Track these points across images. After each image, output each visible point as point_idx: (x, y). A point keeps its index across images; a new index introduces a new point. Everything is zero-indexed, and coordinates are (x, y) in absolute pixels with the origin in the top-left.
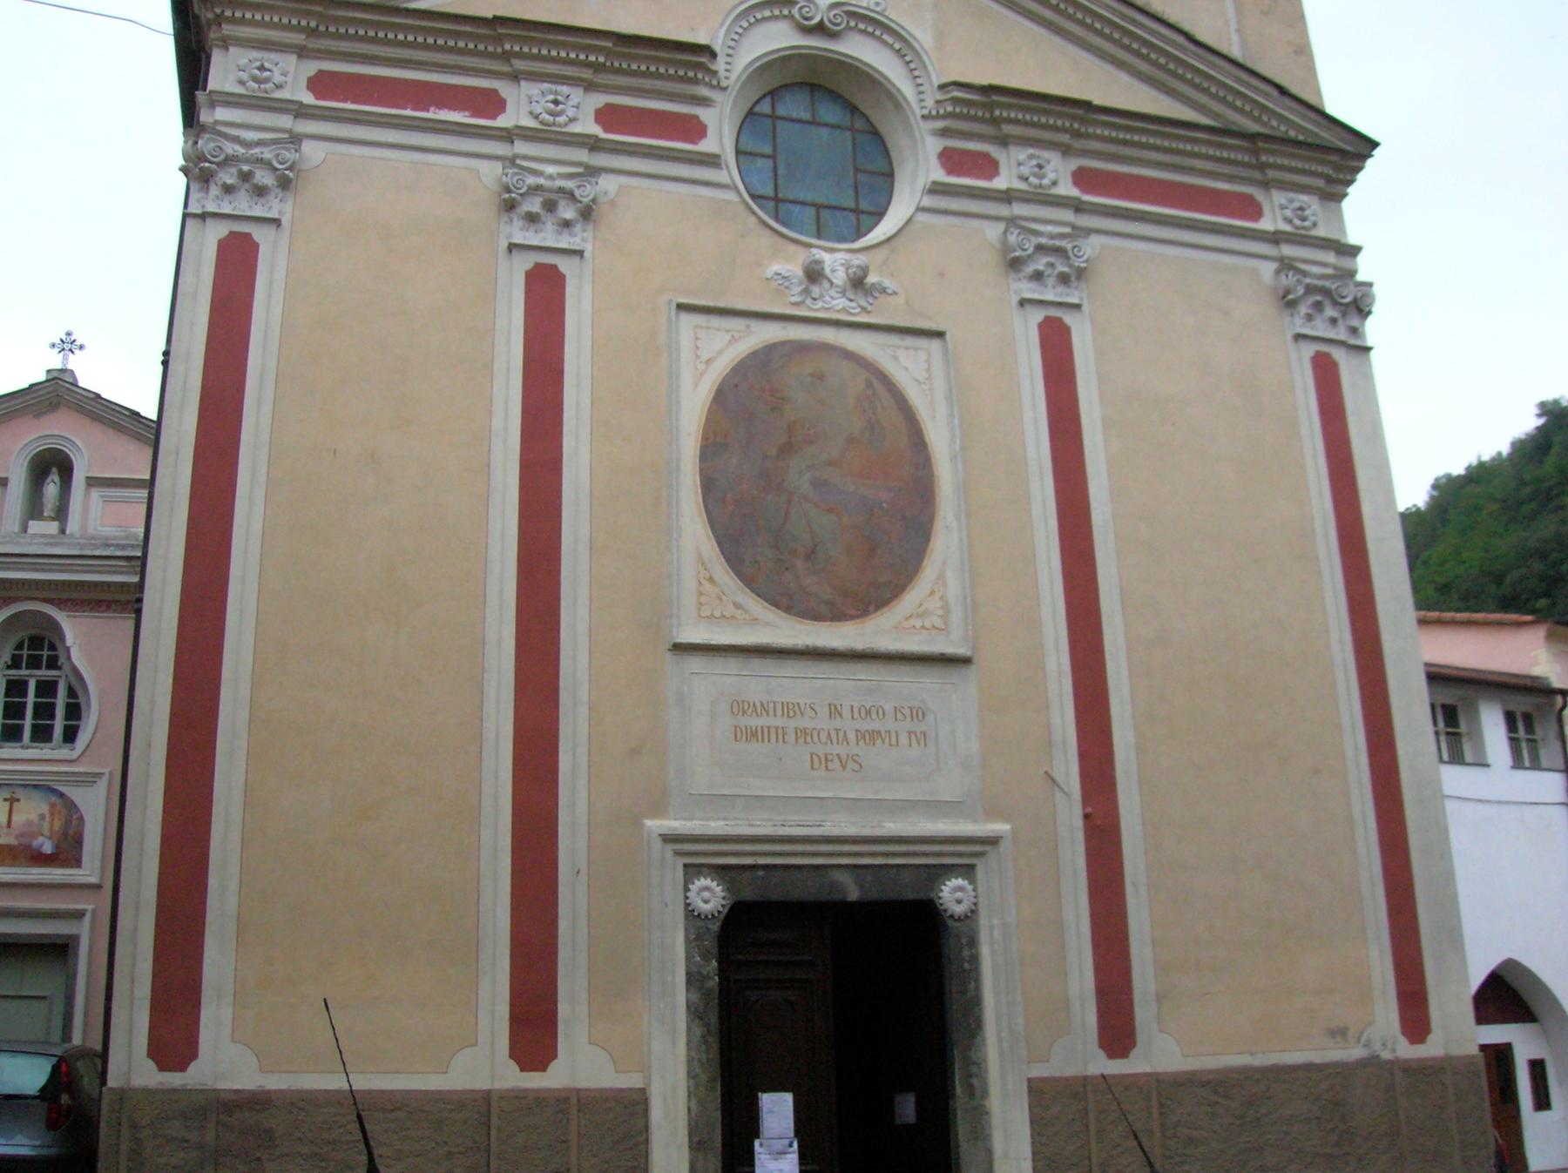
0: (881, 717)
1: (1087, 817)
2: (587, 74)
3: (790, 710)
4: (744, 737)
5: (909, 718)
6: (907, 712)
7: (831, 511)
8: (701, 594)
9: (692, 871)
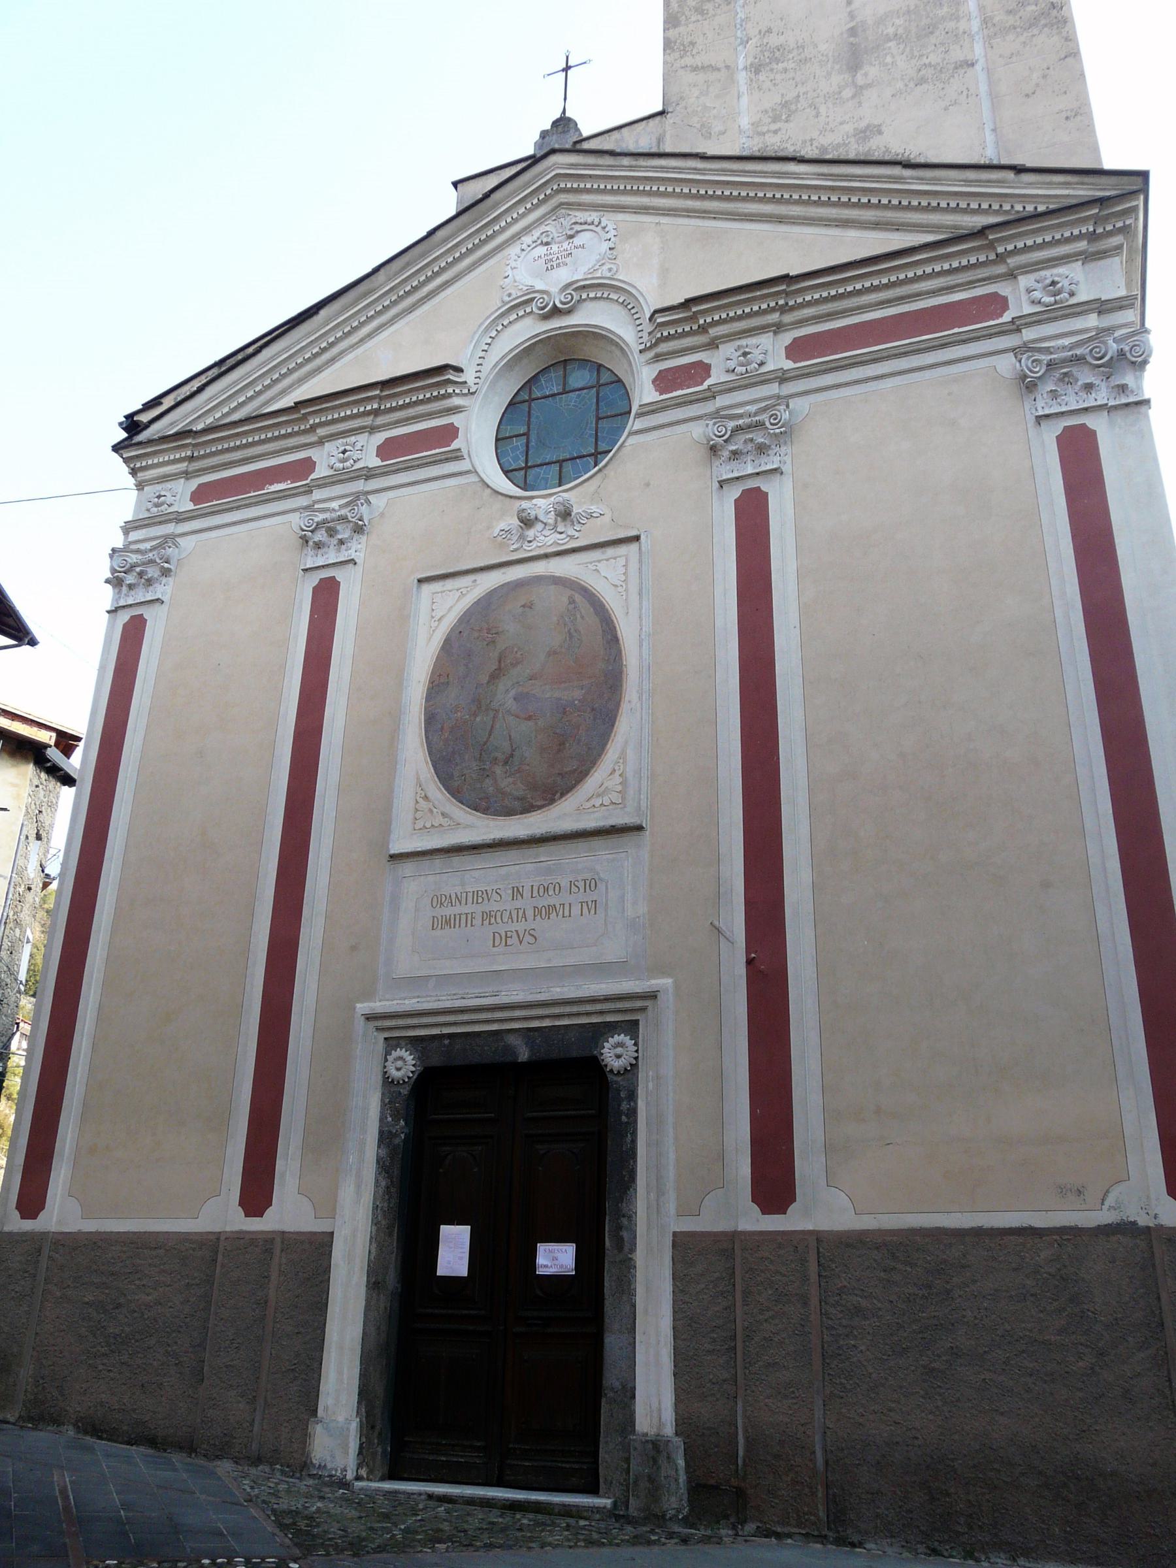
0: (557, 892)
1: (749, 962)
2: (368, 421)
3: (480, 896)
4: (440, 926)
5: (582, 890)
6: (581, 885)
7: (529, 718)
8: (417, 810)
9: (392, 1044)
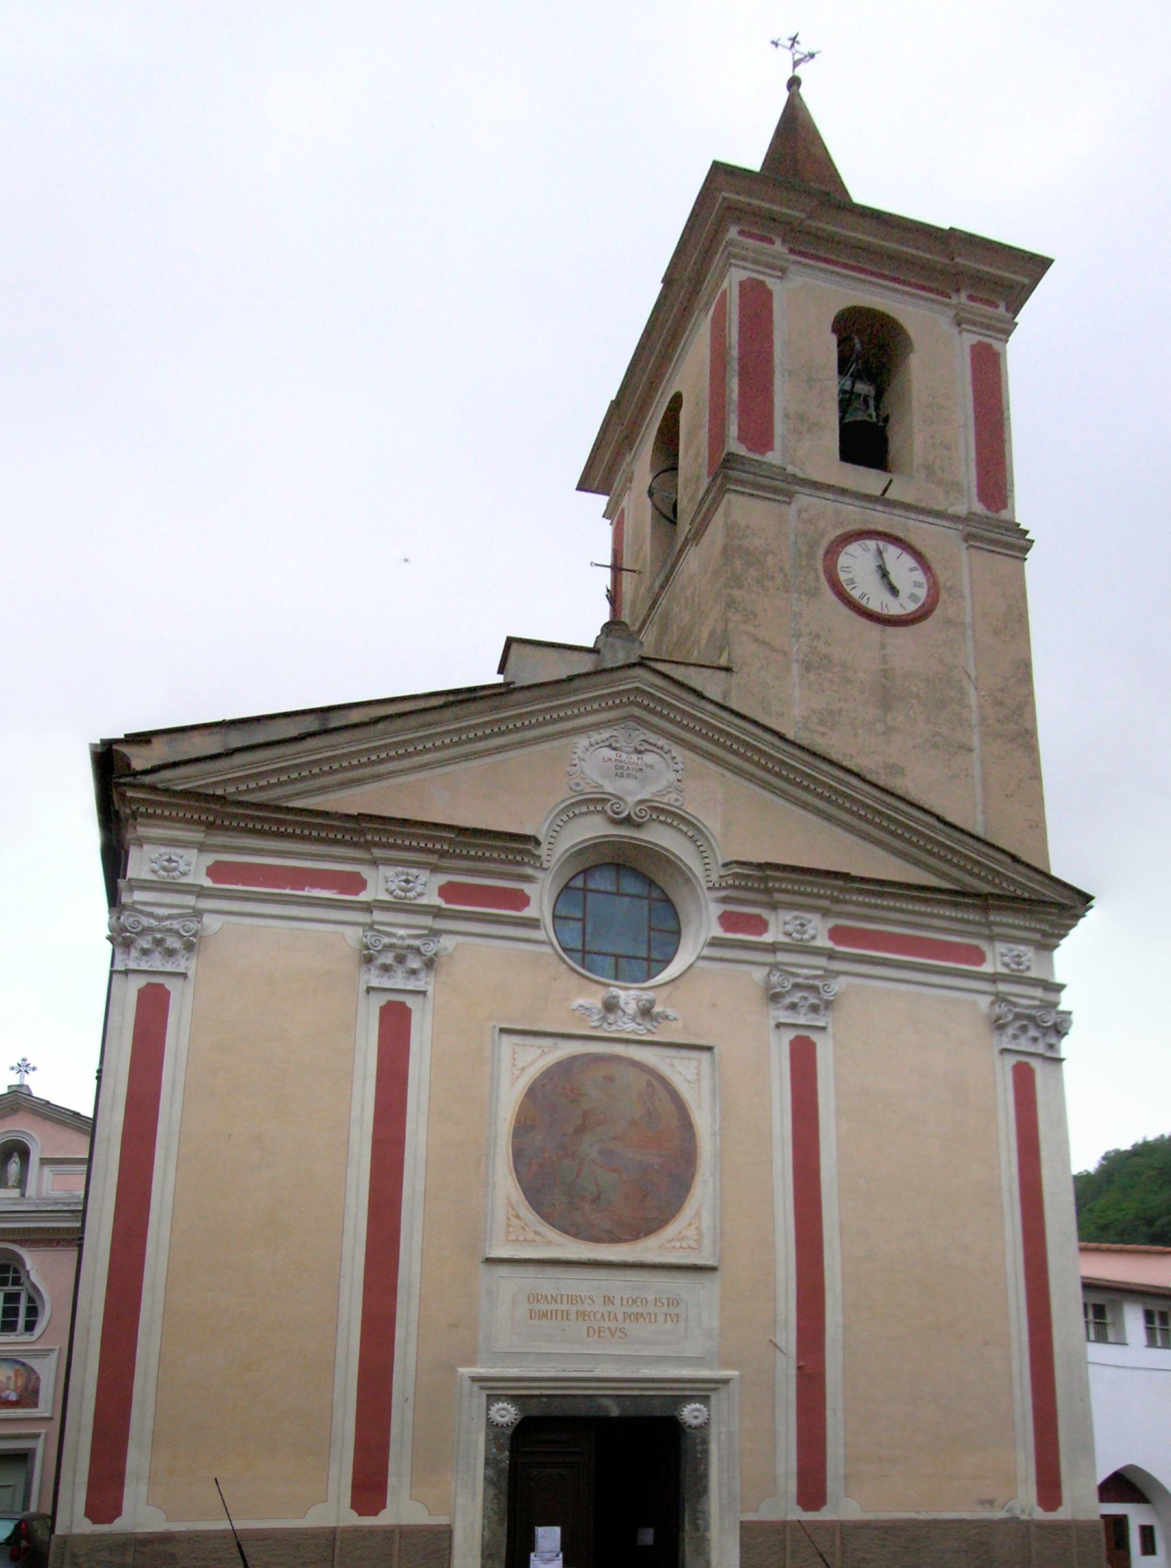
8: (509, 1225)
9: (492, 1399)
